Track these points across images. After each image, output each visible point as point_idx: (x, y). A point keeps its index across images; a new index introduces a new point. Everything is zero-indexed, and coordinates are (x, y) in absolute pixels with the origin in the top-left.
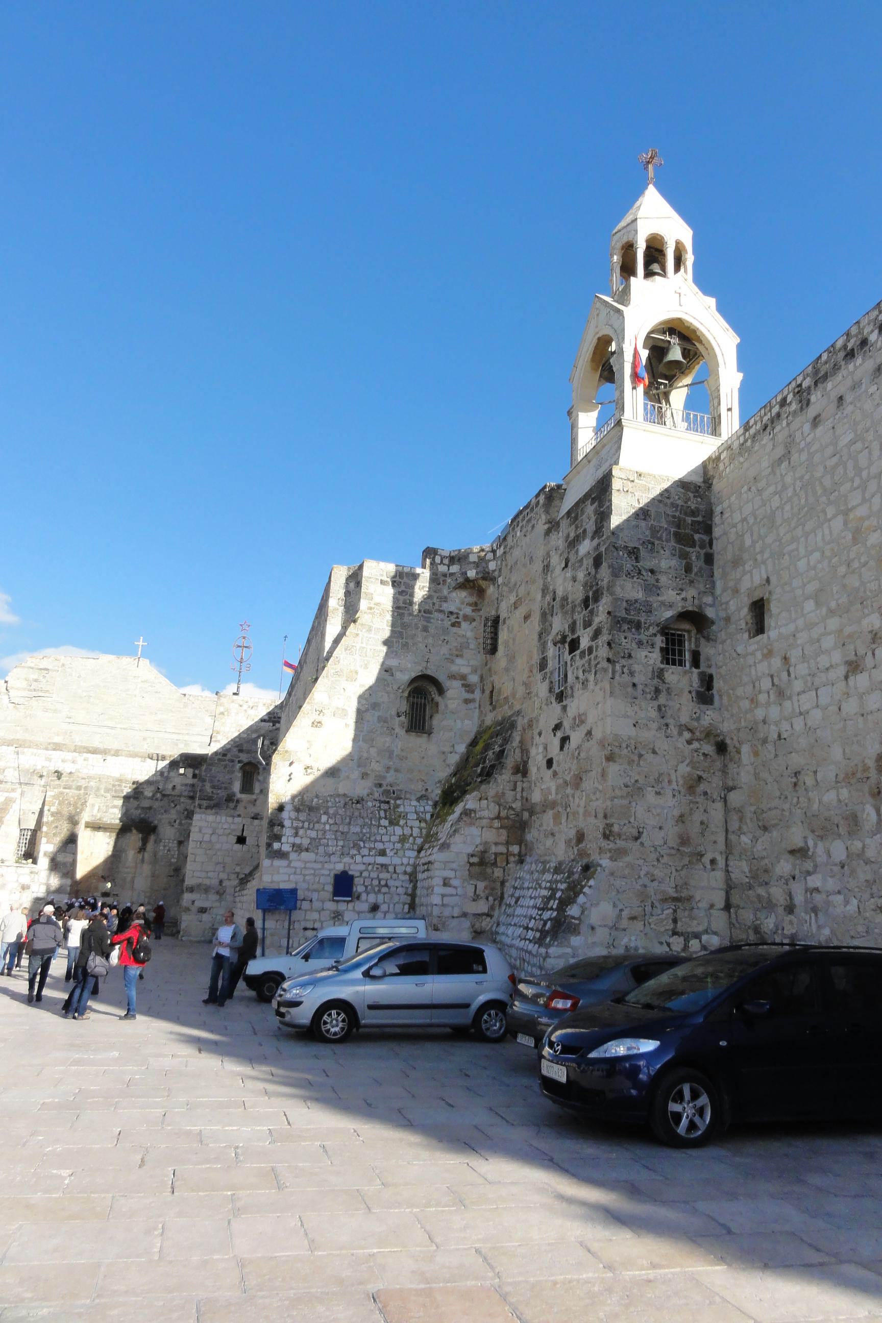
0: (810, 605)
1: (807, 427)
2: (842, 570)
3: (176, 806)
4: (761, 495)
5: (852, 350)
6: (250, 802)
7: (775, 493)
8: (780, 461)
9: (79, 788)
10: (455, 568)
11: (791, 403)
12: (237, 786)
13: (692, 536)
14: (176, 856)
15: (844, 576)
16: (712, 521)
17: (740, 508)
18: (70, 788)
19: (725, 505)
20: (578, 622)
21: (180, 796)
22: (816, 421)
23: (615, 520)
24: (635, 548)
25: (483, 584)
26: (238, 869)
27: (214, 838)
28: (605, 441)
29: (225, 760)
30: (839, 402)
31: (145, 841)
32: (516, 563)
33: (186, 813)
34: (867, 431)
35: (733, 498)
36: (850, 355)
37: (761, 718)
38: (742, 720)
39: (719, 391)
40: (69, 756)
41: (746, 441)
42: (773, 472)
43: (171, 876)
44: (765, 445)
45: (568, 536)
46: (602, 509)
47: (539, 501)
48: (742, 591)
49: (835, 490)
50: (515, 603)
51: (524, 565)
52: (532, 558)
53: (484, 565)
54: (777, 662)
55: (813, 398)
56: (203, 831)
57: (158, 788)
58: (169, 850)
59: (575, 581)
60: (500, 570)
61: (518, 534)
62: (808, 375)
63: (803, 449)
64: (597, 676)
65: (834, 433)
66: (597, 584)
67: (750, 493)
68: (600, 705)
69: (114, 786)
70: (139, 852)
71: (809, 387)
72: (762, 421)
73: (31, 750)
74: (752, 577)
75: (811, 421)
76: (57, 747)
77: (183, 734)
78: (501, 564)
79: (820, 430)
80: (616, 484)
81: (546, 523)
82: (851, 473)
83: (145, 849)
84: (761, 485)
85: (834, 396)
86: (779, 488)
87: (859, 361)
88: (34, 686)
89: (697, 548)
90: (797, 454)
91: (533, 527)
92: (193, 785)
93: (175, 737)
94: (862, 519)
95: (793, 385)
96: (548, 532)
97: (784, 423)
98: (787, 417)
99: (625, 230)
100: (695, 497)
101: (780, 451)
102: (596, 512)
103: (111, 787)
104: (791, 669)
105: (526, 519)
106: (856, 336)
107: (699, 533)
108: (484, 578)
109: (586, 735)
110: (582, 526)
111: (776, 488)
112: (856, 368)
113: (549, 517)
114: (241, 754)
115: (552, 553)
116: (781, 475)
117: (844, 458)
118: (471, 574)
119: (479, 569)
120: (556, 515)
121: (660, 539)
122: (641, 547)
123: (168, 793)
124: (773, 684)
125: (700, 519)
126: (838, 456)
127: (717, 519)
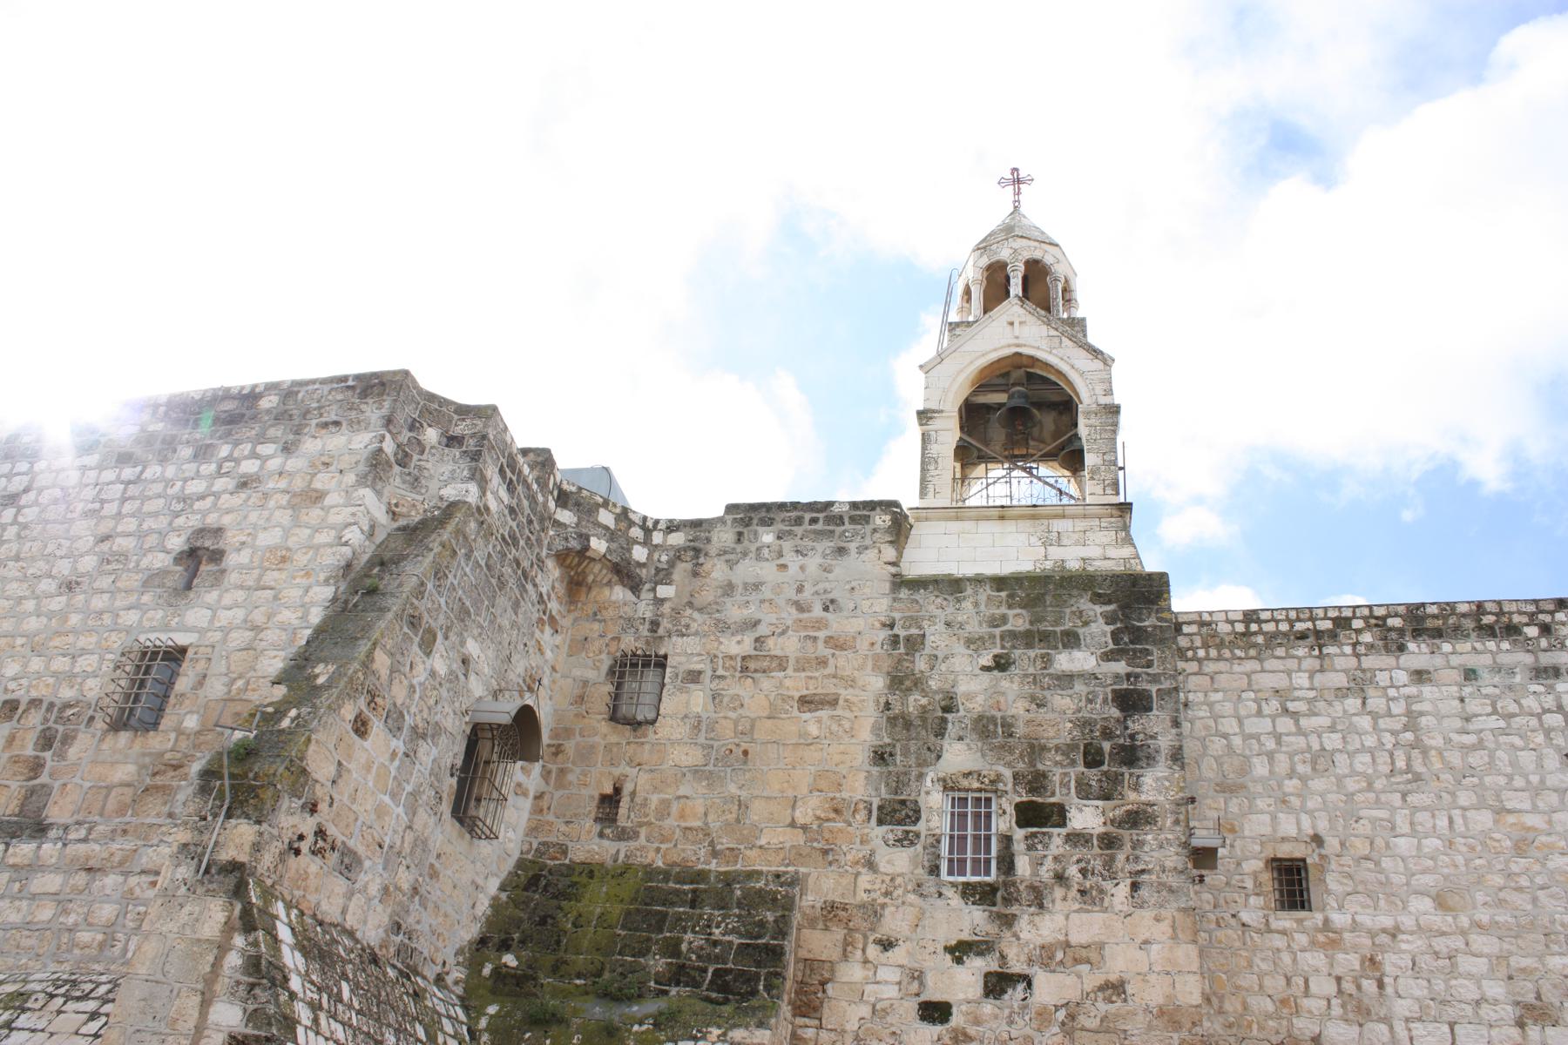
0: (1422, 904)
1: (1402, 677)
2: (1499, 880)
8: (1341, 693)
10: (566, 516)
15: (1500, 889)
20: (1057, 779)
22: (1420, 676)
32: (757, 586)
36: (1489, 632)
37: (1308, 1034)
38: (1255, 1027)
48: (1247, 833)
50: (744, 658)
54: (1348, 962)
55: (1412, 646)
59: (1039, 706)
62: (1396, 615)
64: (1144, 892)
66: (1132, 737)
68: (1155, 947)
71: (1401, 632)
72: (1292, 627)
74: (1274, 818)
79: (1427, 690)
85: (1455, 660)
91: (841, 551)
94: (1529, 829)
95: (1366, 612)
99: (1036, 244)
101: (1340, 680)
104: (1387, 980)
105: (806, 526)
106: (1495, 614)
109: (1101, 988)
110: (1057, 623)
112: (1500, 650)
116: (1345, 711)
118: (598, 545)
119: (614, 546)
124: (1340, 992)
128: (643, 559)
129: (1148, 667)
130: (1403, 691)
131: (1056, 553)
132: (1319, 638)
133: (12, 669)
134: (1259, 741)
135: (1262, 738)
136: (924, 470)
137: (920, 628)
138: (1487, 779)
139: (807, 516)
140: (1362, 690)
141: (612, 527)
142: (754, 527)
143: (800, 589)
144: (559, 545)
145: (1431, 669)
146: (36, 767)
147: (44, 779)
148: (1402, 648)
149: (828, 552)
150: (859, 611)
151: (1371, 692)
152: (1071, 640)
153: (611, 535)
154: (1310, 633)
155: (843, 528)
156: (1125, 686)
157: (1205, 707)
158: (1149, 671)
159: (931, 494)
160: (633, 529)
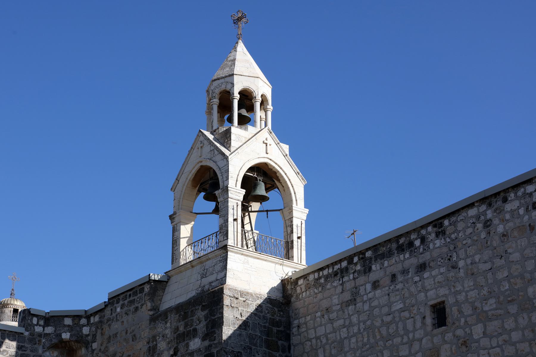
1: (369, 287)
4: (332, 323)
5: (402, 245)
7: (344, 326)
8: (348, 303)
10: (49, 330)
11: (356, 264)
13: (277, 342)
16: (290, 330)
17: (315, 328)
19: (302, 320)
22: (376, 285)
23: (227, 331)
24: (239, 352)
25: (75, 345)
28: (210, 256)
30: (392, 278)
32: (116, 335)
34: (413, 306)
35: (308, 318)
36: (401, 249)
39: (292, 222)
41: (320, 278)
42: (342, 309)
44: (335, 287)
45: (177, 329)
46: (213, 318)
47: (143, 288)
49: (390, 340)
51: (126, 340)
52: (134, 335)
53: (78, 329)
55: (374, 267)
60: (94, 336)
61: (118, 310)
63: (366, 301)
65: (389, 299)
67: (323, 319)
71: (371, 258)
72: (333, 268)
75: (372, 282)
78: (96, 331)
79: (378, 292)
80: (227, 301)
81: (150, 310)
82: (402, 333)
84: (333, 315)
85: (389, 271)
86: (347, 323)
87: (407, 255)
89: (280, 353)
90: (361, 304)
91: (137, 309)
96: (153, 319)
97: (351, 276)
98: (354, 273)
99: (222, 80)
100: (279, 311)
101: (347, 296)
102: (206, 317)
105: (128, 300)
107: (282, 340)
108: (77, 341)
110: (192, 325)
111: (345, 322)
113: (153, 305)
115: (158, 338)
116: (349, 314)
117: (397, 319)
118: (66, 336)
120: (159, 302)
121: (255, 345)
122: (243, 352)
125: (281, 329)
126: (392, 315)
127: (294, 330)
128: (88, 333)
129: (215, 340)
130: (370, 295)
131: (206, 281)
132: (344, 272)
134: (320, 340)
135: (322, 338)
136: (173, 248)
137: (156, 341)
138: (395, 340)
139: (128, 294)
140: (355, 300)
141: (71, 324)
142: (115, 305)
143: (126, 333)
144: (47, 344)
145: (379, 279)
148: (370, 269)
149: (133, 310)
150: (141, 338)
151: (358, 300)
152: (194, 333)
153: (70, 328)
154: (339, 271)
155: (137, 296)
156: (207, 353)
157: (304, 326)
158: (215, 342)
159: (175, 261)
160: (82, 320)
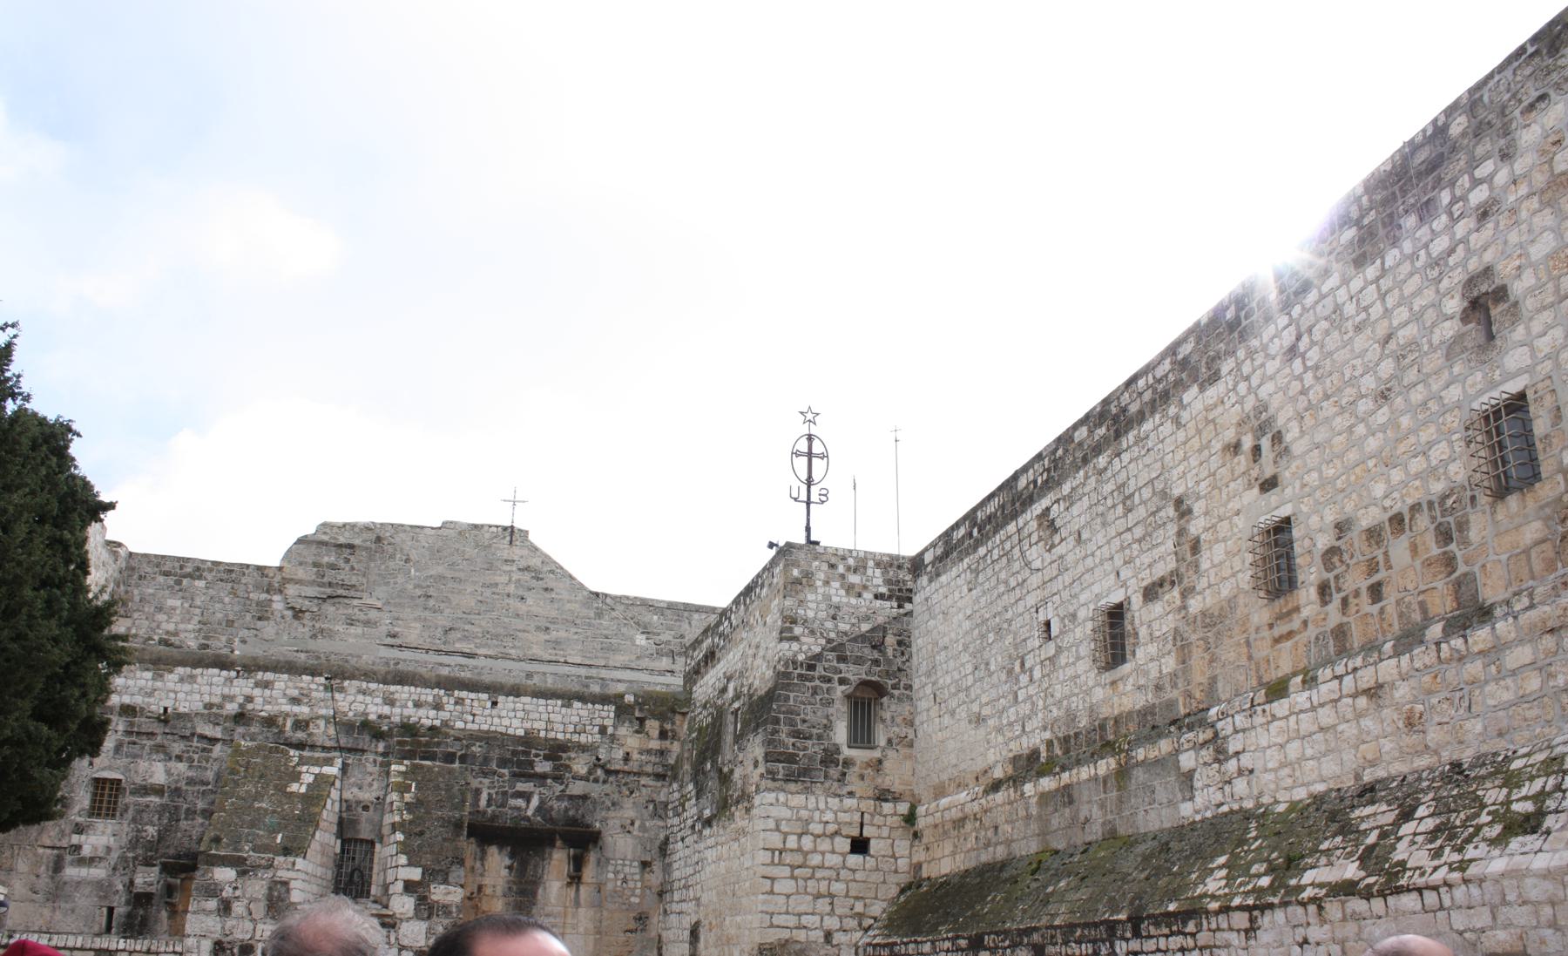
3: (632, 793)
6: (868, 765)
9: (449, 758)
12: (841, 733)
14: (638, 892)
18: (432, 757)
21: (639, 774)
26: (859, 907)
27: (807, 842)
29: (812, 679)
31: (578, 863)
33: (651, 807)
40: (428, 695)
43: (631, 931)
56: (784, 828)
57: (598, 759)
58: (625, 881)
69: (514, 753)
70: (569, 884)
73: (355, 683)
76: (402, 679)
77: (598, 667)
83: (579, 878)
88: (330, 576)
92: (662, 753)
93: (583, 671)
103: (508, 756)
114: (842, 666)
123: (618, 767)
133: (1379, 489)
146: (1449, 562)
147: (1462, 569)
